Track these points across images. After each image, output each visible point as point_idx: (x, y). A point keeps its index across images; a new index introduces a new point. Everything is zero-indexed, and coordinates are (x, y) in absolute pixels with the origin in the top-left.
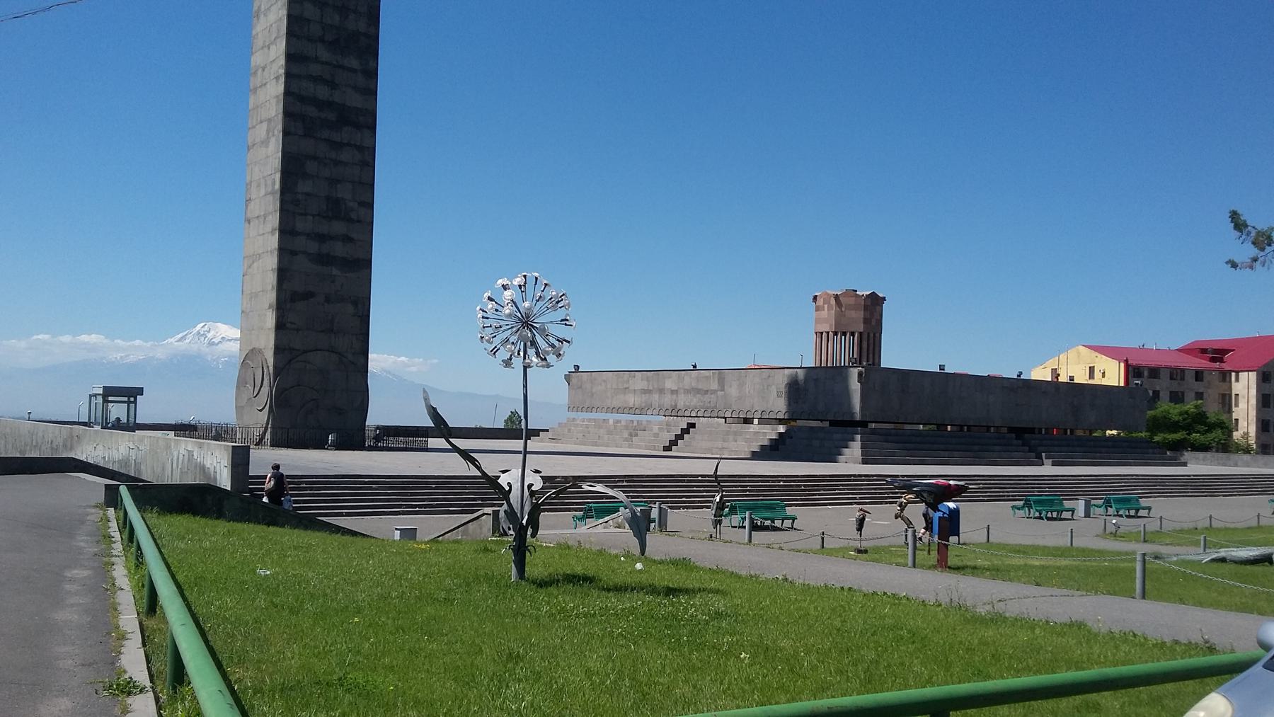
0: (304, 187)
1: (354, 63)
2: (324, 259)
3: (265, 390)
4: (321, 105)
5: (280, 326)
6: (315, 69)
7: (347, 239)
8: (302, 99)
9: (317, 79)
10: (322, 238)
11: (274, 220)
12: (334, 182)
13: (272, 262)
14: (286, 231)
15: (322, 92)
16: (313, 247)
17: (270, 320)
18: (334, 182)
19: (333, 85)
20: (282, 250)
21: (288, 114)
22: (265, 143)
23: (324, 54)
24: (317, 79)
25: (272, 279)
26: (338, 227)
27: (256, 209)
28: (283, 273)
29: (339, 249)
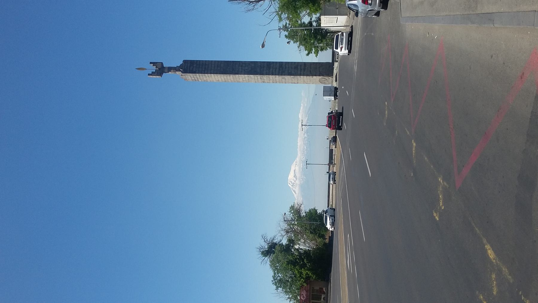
0: (293, 72)
1: (272, 65)
2: (304, 70)
3: (326, 78)
4: (279, 70)
5: (316, 76)
6: (274, 71)
7: (301, 66)
8: (279, 73)
9: (275, 71)
10: (301, 70)
11: (298, 77)
12: (292, 68)
13: (305, 77)
14: (300, 75)
15: (277, 70)
16: (303, 71)
17: (315, 77)
18: (292, 68)
19: (276, 69)
20: (303, 75)
21: (282, 75)
22: (286, 79)
23: (271, 70)
24: (275, 71)
25: (308, 77)
26: (299, 67)
27: (296, 81)
28: (307, 75)
29: (303, 67)
